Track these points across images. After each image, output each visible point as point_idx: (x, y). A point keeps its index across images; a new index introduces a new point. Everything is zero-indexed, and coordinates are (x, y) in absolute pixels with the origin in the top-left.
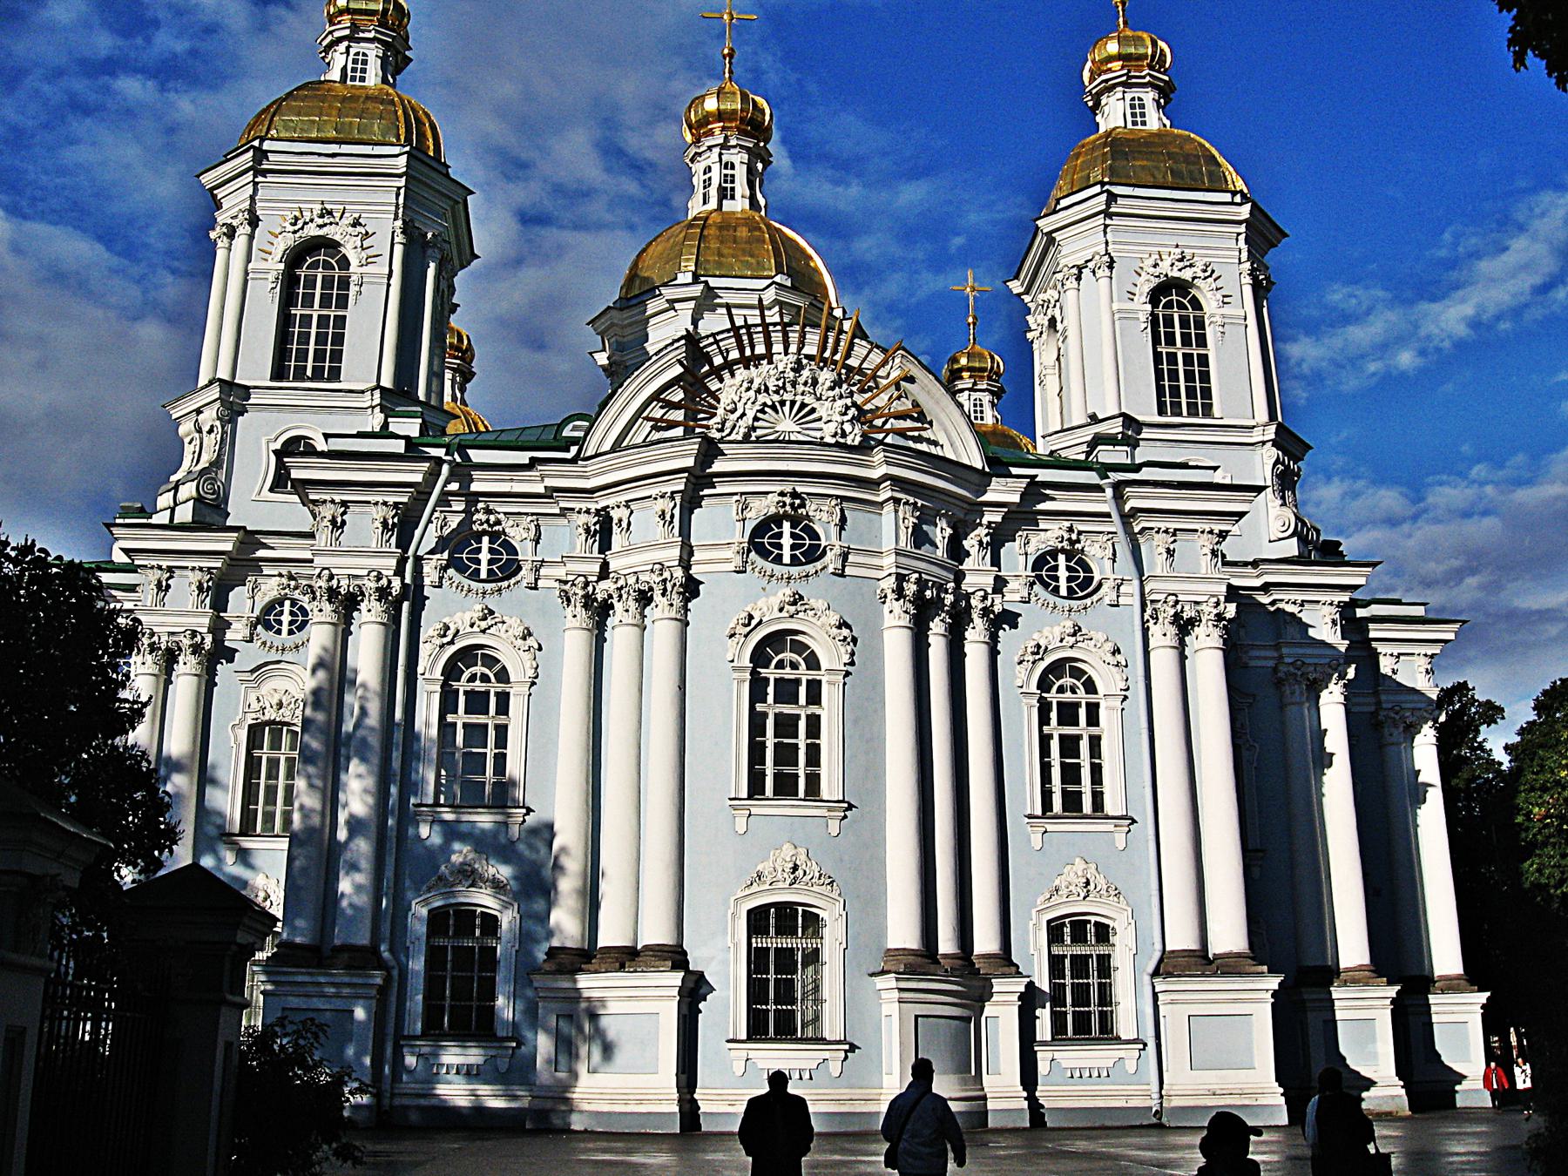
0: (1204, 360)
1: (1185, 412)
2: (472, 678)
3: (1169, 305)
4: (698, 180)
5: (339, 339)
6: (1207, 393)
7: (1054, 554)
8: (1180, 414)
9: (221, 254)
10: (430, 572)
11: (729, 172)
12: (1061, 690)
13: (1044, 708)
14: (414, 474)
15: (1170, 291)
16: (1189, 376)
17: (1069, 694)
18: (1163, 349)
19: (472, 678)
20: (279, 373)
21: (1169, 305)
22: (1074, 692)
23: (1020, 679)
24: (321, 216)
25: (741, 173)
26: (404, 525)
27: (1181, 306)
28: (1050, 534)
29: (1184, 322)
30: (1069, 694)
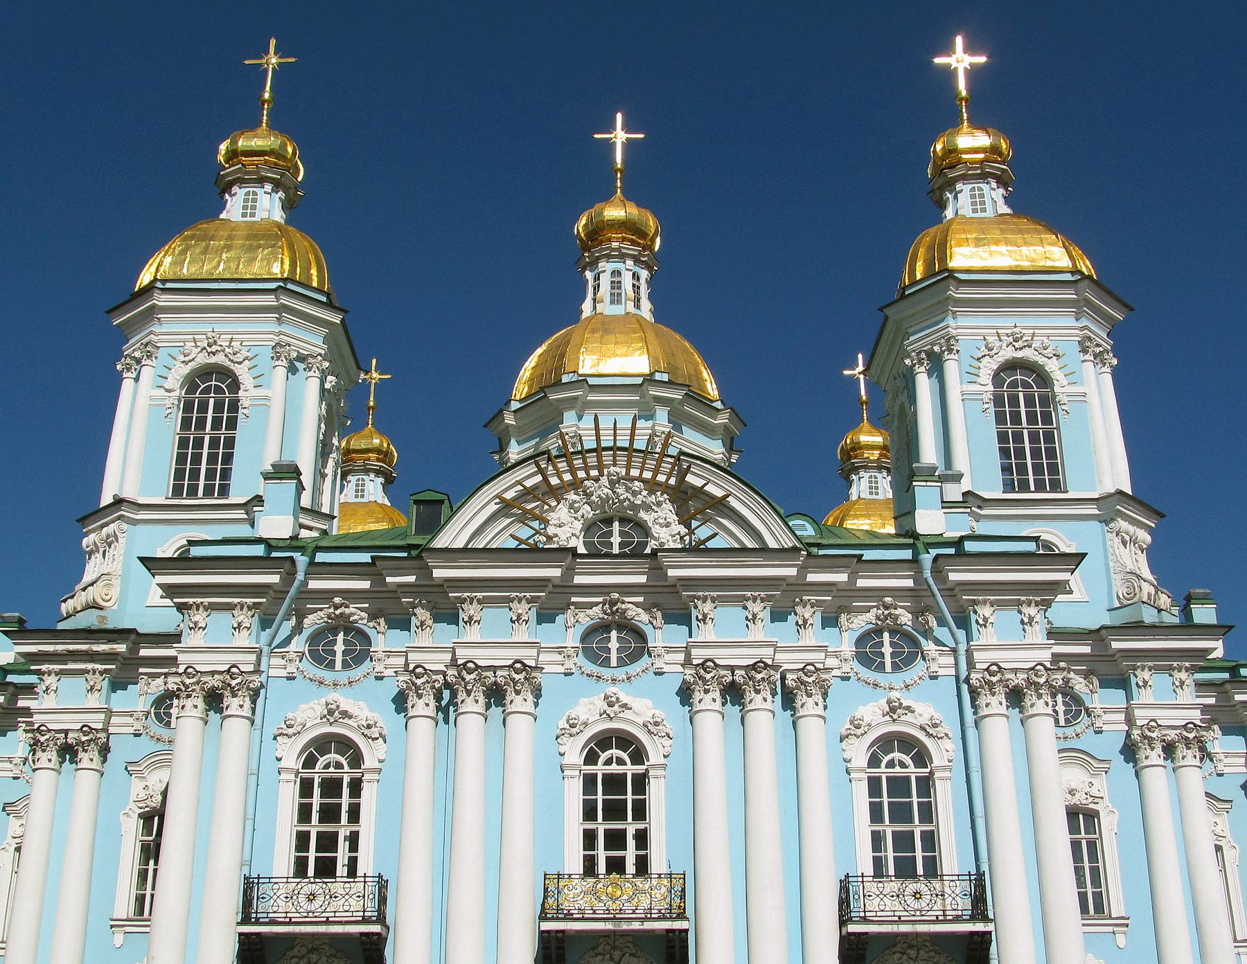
0: (1049, 437)
1: (1032, 488)
6: (1053, 469)
8: (1028, 490)
12: (891, 764)
16: (1036, 453)
17: (898, 769)
18: (1010, 428)
19: (327, 766)
21: (1014, 384)
22: (902, 765)
24: (210, 345)
25: (627, 281)
27: (1026, 385)
29: (1029, 402)
30: (898, 769)
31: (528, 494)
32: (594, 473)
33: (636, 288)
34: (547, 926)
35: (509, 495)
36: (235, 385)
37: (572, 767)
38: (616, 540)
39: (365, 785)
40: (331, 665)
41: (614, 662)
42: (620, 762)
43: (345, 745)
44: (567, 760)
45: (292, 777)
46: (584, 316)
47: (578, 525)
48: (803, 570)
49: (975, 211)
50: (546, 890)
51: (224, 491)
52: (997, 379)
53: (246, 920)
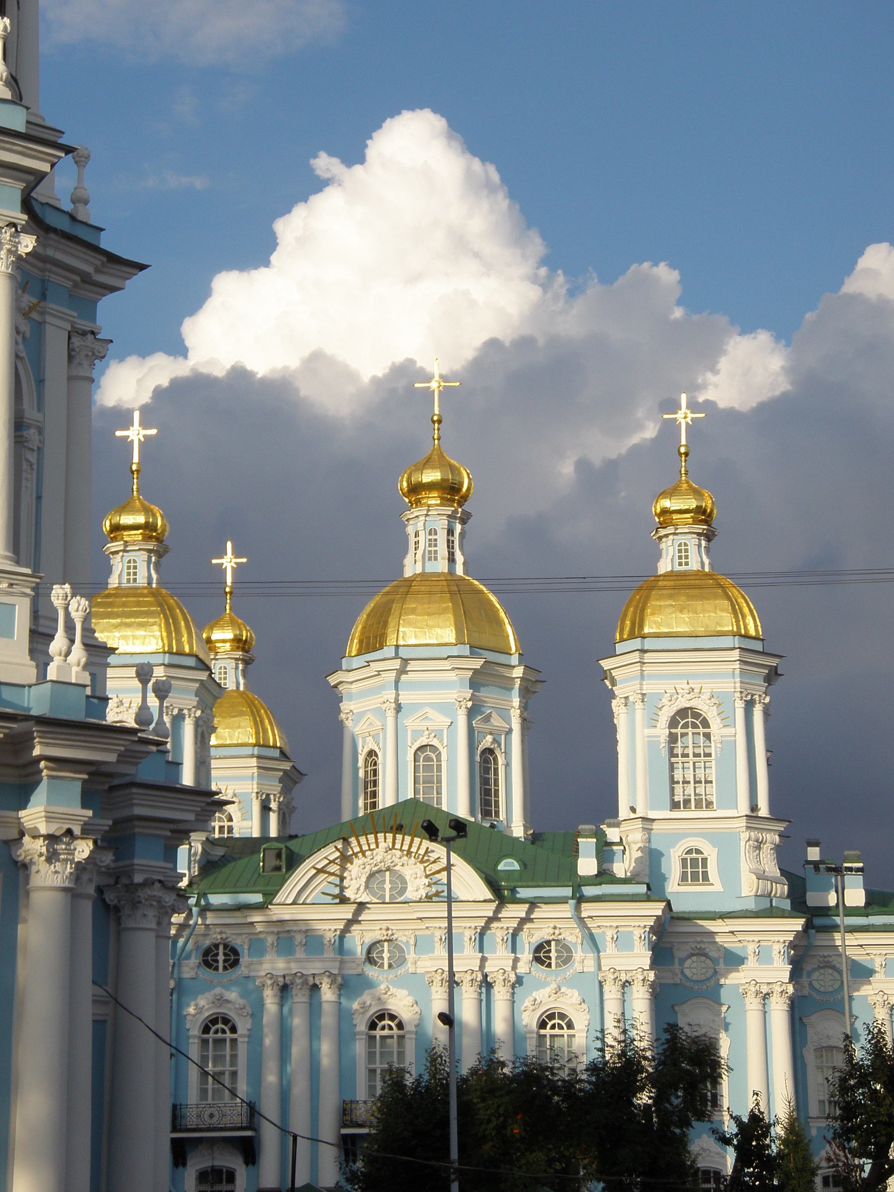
2: (216, 1032)
3: (686, 726)
4: (412, 540)
11: (433, 537)
12: (553, 1027)
15: (686, 717)
25: (442, 537)
27: (695, 726)
32: (373, 846)
33: (450, 545)
34: (344, 1131)
35: (319, 866)
37: (360, 1033)
38: (387, 886)
39: (240, 1045)
40: (217, 969)
41: (386, 966)
42: (391, 1028)
43: (226, 1021)
44: (358, 1029)
45: (196, 1041)
46: (408, 573)
47: (364, 879)
49: (680, 564)
50: (345, 1110)
52: (673, 723)
53: (174, 1129)
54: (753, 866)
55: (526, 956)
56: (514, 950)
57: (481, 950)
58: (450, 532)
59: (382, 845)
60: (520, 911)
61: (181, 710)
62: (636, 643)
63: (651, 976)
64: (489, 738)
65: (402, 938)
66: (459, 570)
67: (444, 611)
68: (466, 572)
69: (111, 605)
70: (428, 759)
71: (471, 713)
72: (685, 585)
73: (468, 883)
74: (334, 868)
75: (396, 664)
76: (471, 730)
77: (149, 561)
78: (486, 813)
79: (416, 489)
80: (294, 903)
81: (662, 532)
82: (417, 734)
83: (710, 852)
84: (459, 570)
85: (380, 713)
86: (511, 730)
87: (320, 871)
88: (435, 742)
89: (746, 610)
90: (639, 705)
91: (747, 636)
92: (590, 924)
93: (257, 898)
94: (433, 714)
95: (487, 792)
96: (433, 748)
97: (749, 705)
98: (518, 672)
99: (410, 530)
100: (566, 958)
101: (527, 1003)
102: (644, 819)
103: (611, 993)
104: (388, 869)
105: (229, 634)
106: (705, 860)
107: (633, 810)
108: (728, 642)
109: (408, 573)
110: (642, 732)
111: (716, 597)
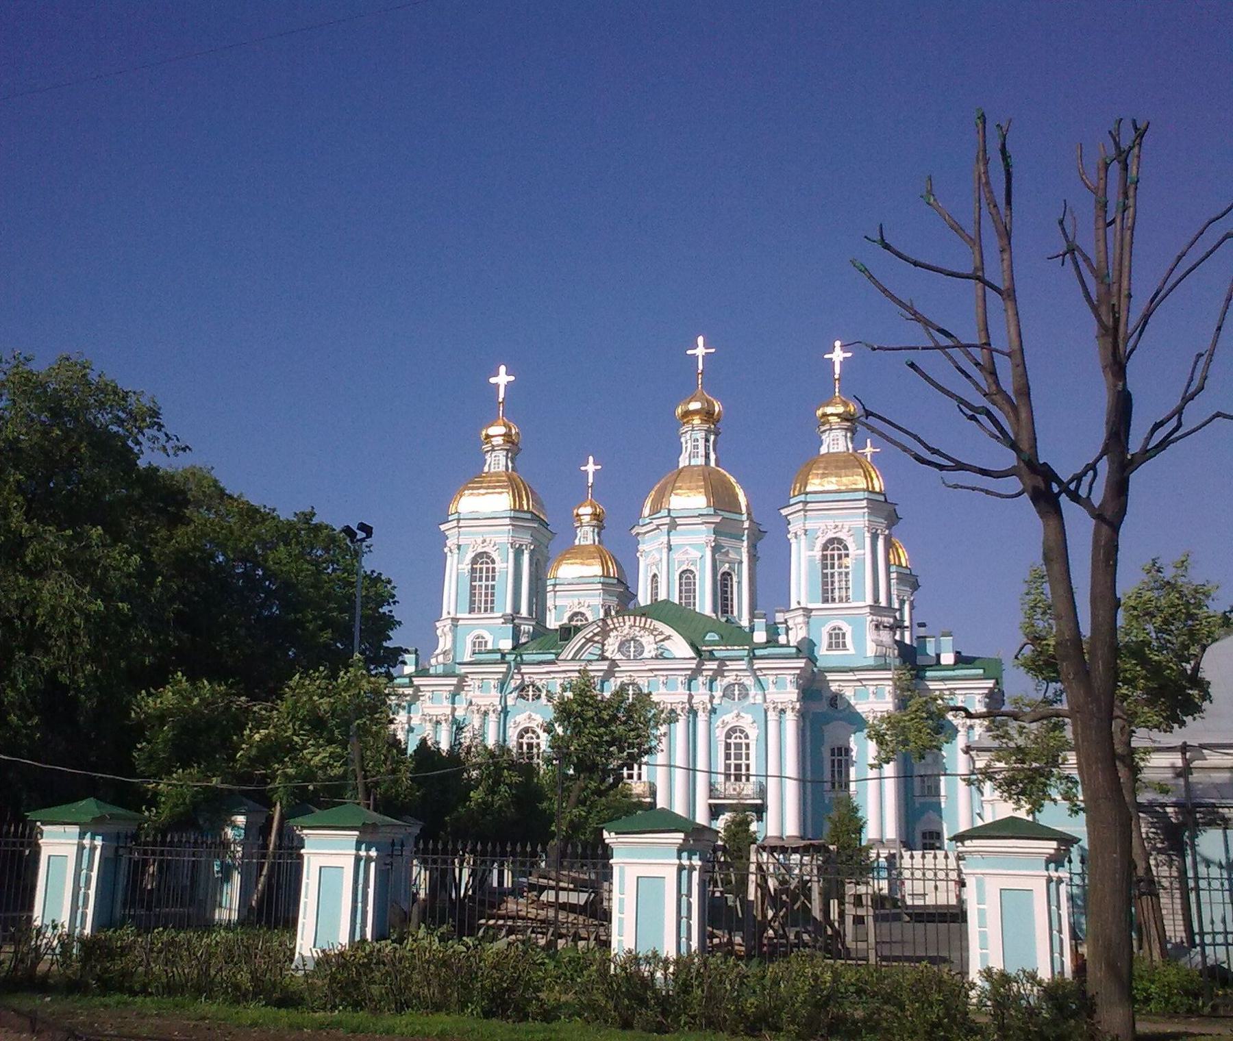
5: (493, 594)
7: (734, 685)
9: (449, 559)
10: (510, 702)
13: (728, 746)
14: (503, 668)
20: (471, 610)
23: (720, 734)
25: (701, 443)
26: (502, 685)
27: (839, 549)
28: (730, 678)
31: (596, 635)
33: (707, 448)
36: (493, 562)
38: (632, 649)
46: (681, 465)
48: (700, 664)
51: (492, 608)
52: (825, 548)
54: (875, 637)
55: (718, 693)
56: (711, 690)
57: (689, 689)
58: (707, 440)
59: (628, 624)
60: (713, 665)
61: (521, 545)
62: (802, 498)
63: (798, 706)
64: (727, 565)
65: (640, 682)
66: (713, 464)
67: (698, 487)
68: (717, 465)
69: (481, 482)
70: (688, 578)
71: (716, 549)
72: (839, 464)
73: (680, 647)
74: (596, 638)
75: (667, 520)
76: (714, 561)
77: (507, 457)
78: (725, 612)
79: (687, 414)
80: (572, 659)
81: (823, 428)
82: (681, 563)
83: (847, 629)
84: (713, 464)
85: (660, 551)
86: (741, 562)
87: (588, 640)
88: (692, 568)
89: (873, 475)
90: (803, 537)
91: (873, 492)
92: (759, 673)
93: (553, 657)
94: (690, 550)
95: (726, 599)
96: (692, 572)
97: (874, 537)
98: (746, 525)
99: (683, 440)
100: (744, 694)
101: (719, 723)
102: (805, 609)
103: (772, 716)
104: (632, 639)
105: (589, 510)
106: (844, 634)
107: (799, 603)
108: (861, 495)
109: (681, 465)
110: (805, 554)
111: (854, 467)
